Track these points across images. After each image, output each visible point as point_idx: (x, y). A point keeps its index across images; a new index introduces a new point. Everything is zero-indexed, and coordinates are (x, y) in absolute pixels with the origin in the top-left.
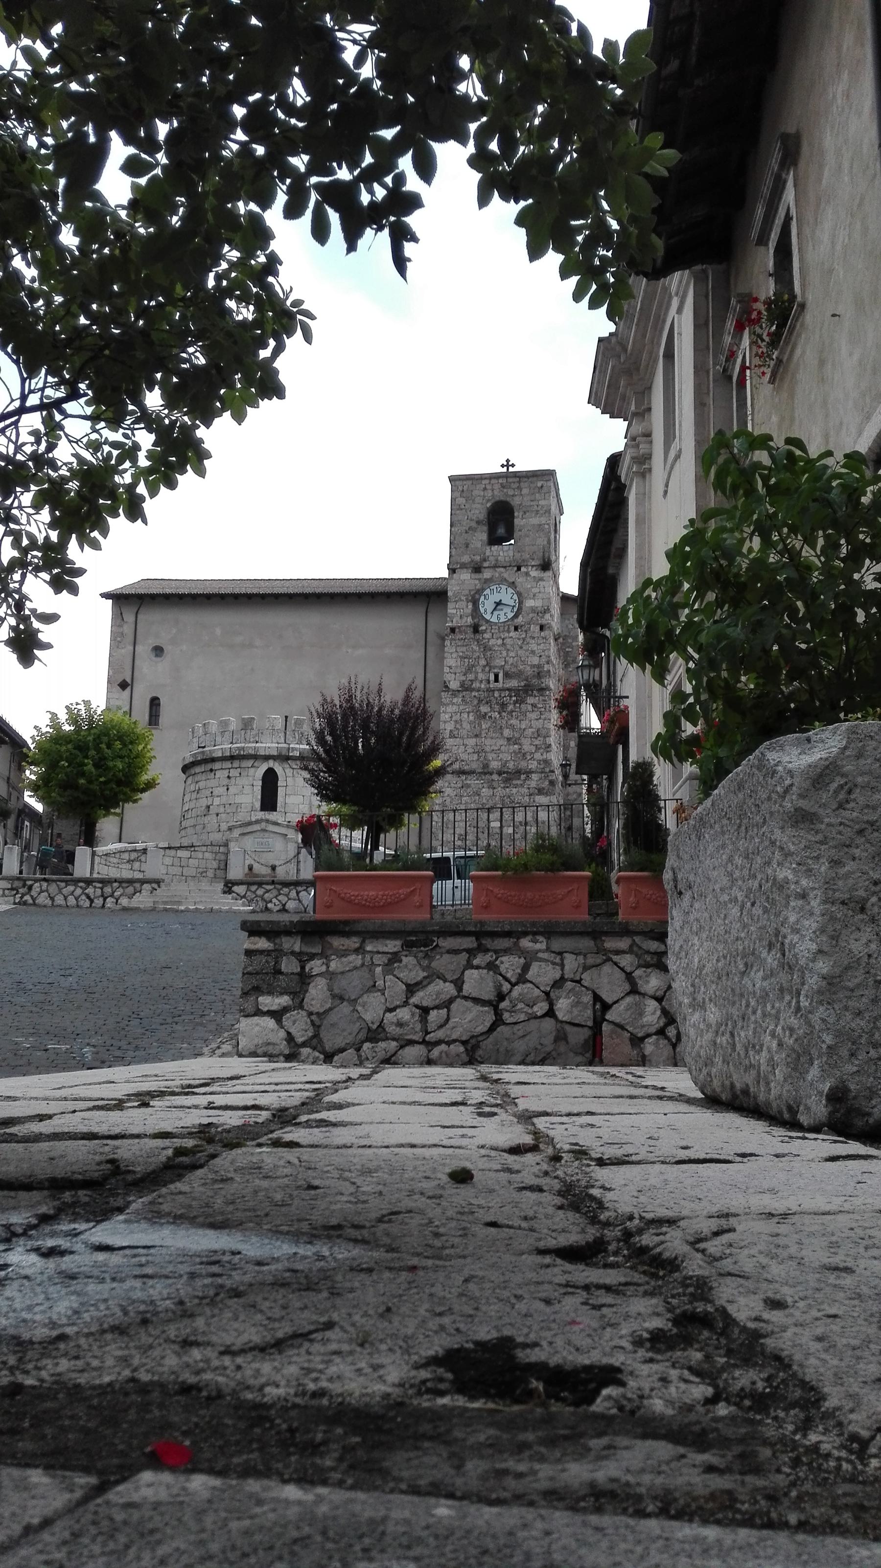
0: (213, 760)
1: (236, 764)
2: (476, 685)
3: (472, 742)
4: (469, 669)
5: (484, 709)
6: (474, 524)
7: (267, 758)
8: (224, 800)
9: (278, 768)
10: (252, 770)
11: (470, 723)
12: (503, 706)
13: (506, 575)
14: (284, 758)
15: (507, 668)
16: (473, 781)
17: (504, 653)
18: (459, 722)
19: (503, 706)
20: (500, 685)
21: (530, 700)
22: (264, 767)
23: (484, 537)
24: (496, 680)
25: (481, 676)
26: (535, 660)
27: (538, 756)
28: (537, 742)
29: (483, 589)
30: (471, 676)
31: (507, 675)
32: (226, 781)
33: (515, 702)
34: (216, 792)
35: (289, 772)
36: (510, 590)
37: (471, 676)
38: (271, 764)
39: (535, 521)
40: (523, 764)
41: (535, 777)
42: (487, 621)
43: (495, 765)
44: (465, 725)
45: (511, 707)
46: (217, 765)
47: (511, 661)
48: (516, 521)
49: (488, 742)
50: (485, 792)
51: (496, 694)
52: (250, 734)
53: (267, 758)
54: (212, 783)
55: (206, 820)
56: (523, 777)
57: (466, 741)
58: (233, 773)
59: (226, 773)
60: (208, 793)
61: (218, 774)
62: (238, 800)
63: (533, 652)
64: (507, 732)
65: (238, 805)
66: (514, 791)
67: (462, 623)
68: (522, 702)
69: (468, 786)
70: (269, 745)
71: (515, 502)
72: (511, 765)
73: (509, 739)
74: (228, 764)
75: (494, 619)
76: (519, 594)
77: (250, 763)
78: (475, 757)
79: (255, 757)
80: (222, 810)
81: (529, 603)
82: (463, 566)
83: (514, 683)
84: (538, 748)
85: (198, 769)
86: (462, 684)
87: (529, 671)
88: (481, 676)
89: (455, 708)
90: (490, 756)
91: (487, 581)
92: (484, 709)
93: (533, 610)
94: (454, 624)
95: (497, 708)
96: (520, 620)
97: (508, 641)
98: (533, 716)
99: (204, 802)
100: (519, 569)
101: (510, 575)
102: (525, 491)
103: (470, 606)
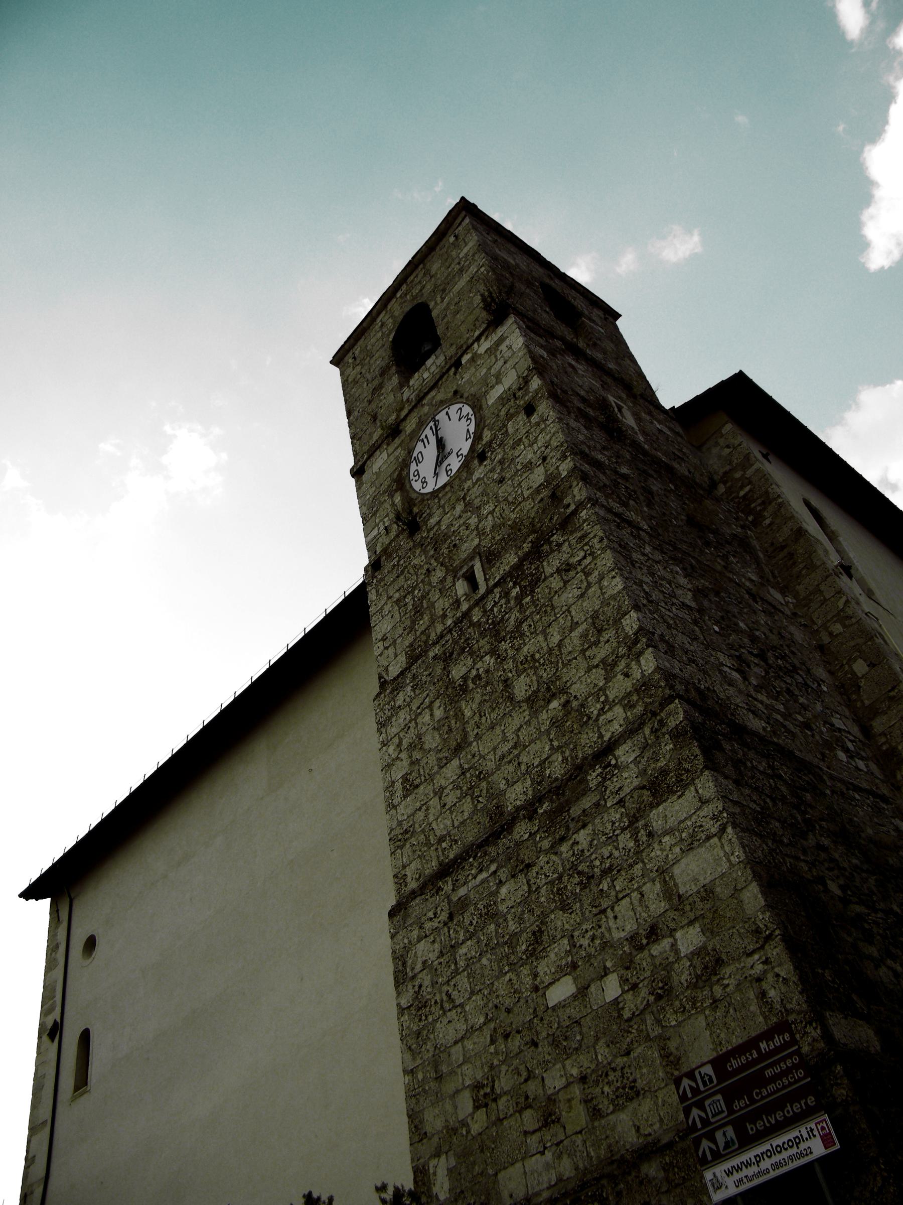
3: (451, 770)
4: (418, 611)
5: (457, 672)
12: (496, 631)
15: (486, 542)
16: (471, 884)
18: (417, 744)
19: (496, 631)
21: (550, 566)
26: (538, 476)
27: (620, 686)
28: (601, 652)
40: (588, 740)
41: (625, 754)
43: (516, 795)
44: (432, 741)
47: (489, 523)
50: (510, 893)
56: (593, 778)
63: (529, 467)
64: (521, 687)
66: (583, 837)
68: (536, 581)
69: (464, 903)
72: (557, 769)
73: (531, 700)
84: (609, 666)
96: (487, 435)
98: (571, 593)
100: (457, 364)
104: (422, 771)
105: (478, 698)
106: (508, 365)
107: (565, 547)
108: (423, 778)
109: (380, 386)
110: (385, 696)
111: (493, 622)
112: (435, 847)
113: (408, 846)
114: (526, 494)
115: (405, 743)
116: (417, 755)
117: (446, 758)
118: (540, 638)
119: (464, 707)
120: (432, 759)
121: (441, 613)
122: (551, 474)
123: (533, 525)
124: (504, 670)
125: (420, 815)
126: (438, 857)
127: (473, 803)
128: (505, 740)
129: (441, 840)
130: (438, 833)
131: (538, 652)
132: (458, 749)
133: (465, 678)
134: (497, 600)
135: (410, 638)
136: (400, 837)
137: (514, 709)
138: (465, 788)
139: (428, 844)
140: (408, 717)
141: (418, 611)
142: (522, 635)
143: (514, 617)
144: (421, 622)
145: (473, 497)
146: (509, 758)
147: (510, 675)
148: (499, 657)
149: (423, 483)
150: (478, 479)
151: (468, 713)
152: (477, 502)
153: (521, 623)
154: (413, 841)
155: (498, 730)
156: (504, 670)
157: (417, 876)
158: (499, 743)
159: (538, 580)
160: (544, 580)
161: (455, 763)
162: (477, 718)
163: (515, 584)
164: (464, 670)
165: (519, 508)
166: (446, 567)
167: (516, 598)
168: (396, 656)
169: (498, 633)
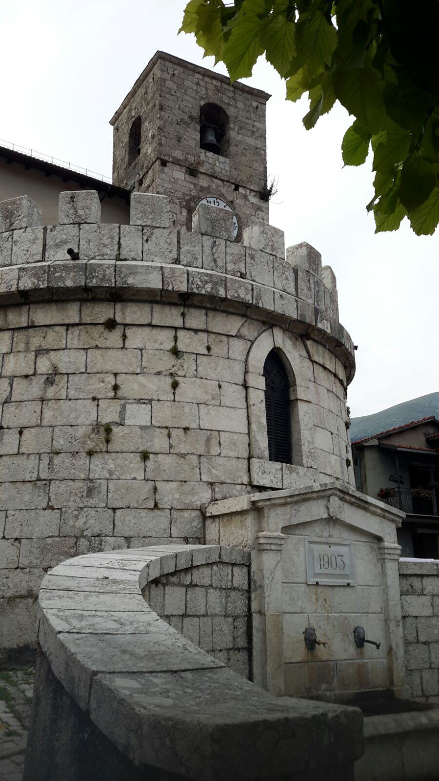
1: (196, 319)
7: (271, 321)
8: (164, 414)
10: (238, 348)
13: (223, 190)
29: (200, 199)
32: (167, 362)
34: (131, 387)
46: (133, 313)
53: (271, 321)
54: (114, 360)
55: (99, 467)
59: (165, 339)
60: (103, 388)
61: (136, 338)
62: (212, 419)
65: (212, 436)
71: (231, 111)
77: (233, 325)
80: (159, 442)
82: (177, 162)
85: (43, 315)
91: (202, 189)
99: (86, 415)
100: (236, 188)
101: (227, 190)
102: (240, 105)
103: (185, 213)
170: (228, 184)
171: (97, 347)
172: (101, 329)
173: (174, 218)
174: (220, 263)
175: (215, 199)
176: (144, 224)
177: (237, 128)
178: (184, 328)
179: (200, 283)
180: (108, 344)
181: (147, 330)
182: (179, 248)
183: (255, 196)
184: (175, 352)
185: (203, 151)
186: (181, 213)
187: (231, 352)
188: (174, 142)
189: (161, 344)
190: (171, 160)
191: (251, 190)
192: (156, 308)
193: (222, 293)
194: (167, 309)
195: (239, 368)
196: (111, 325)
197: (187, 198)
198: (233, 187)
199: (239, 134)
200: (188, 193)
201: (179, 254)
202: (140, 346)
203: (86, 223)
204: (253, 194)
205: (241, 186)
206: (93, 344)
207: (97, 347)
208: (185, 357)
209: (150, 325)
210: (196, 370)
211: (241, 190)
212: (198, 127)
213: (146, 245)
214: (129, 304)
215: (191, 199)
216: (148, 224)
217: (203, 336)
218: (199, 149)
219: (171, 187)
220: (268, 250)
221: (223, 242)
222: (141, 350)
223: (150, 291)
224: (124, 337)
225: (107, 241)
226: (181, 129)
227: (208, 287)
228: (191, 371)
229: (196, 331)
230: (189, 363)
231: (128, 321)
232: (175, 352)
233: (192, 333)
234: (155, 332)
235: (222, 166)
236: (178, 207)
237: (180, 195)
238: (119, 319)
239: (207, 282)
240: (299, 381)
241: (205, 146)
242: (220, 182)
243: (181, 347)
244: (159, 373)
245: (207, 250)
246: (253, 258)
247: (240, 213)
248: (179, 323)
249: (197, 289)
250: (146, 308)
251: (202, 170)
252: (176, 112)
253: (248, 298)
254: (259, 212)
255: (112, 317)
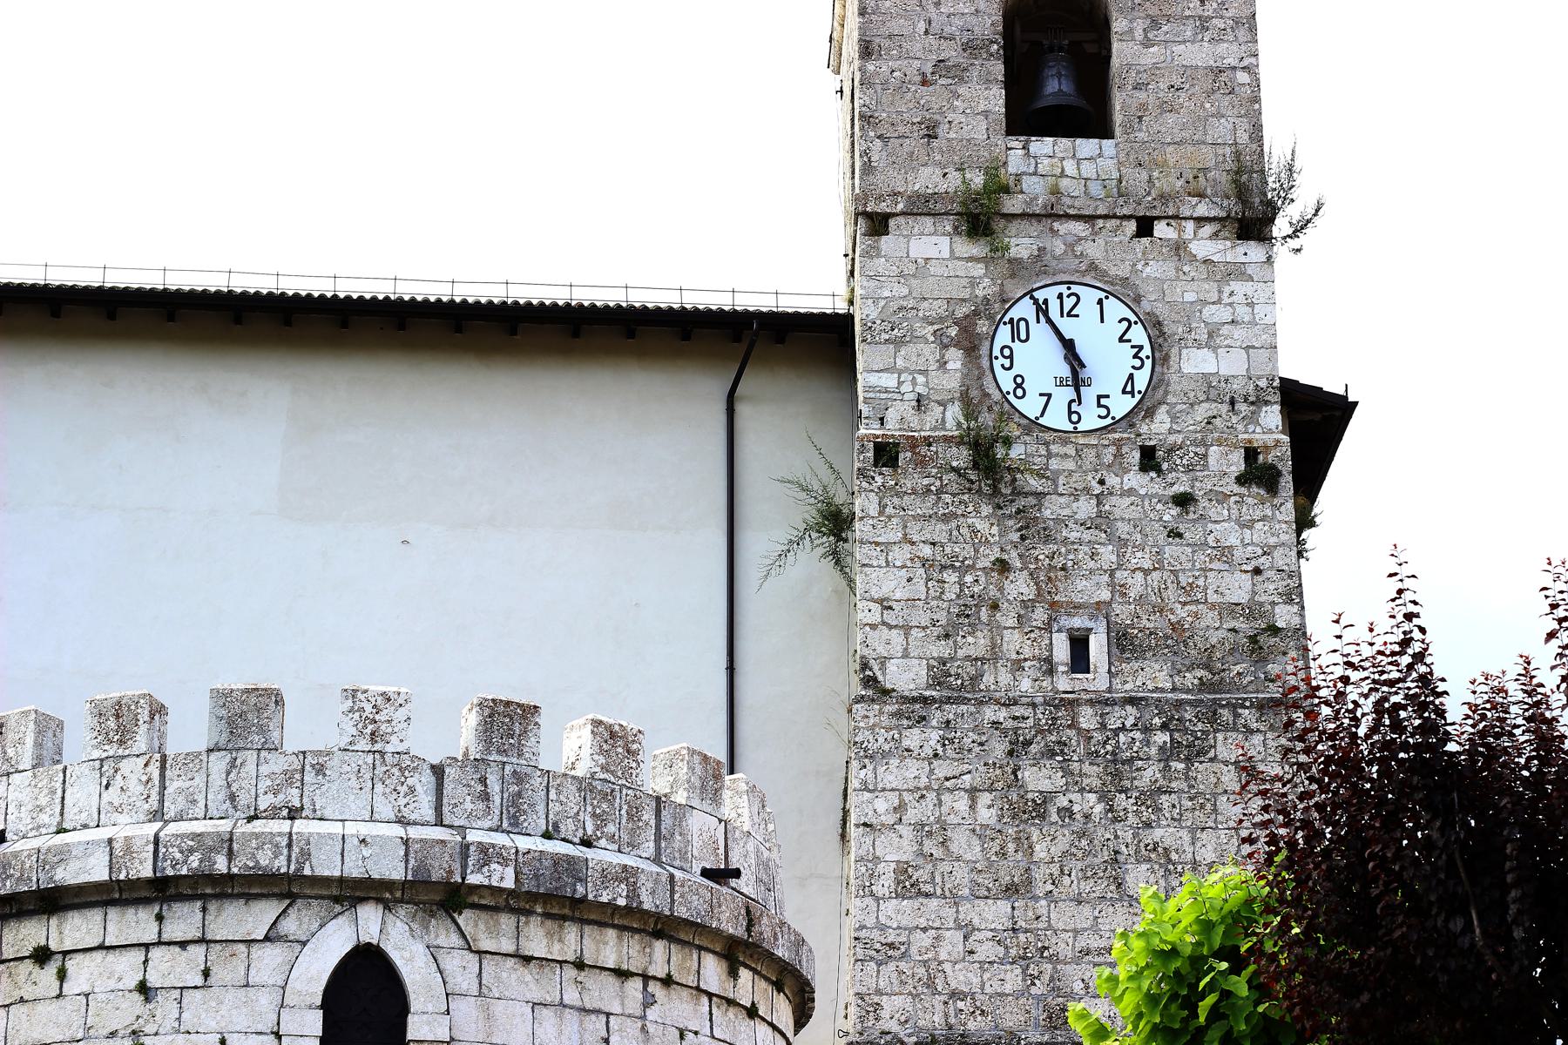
0: (54, 901)
1: (184, 920)
2: (997, 679)
3: (996, 913)
4: (965, 616)
5: (1038, 778)
6: (952, 53)
7: (350, 893)
9: (407, 945)
10: (269, 959)
11: (980, 833)
12: (1118, 768)
13: (1095, 250)
14: (440, 897)
15: (1122, 613)
17: (1108, 555)
19: (1118, 768)
20: (1097, 680)
22: (333, 942)
23: (996, 100)
24: (1080, 660)
25: (1013, 642)
26: (1238, 588)
29: (1007, 302)
30: (977, 644)
31: (1122, 643)
33: (1167, 754)
35: (461, 968)
36: (1115, 309)
37: (977, 644)
38: (370, 923)
39: (1199, 54)
42: (1032, 426)
44: (960, 841)
45: (1150, 774)
46: (76, 929)
48: (1122, 53)
49: (1064, 916)
51: (1087, 718)
52: (259, 775)
53: (350, 893)
57: (968, 912)
58: (167, 968)
59: (127, 967)
61: (82, 972)
63: (1224, 553)
67: (925, 425)
68: (1196, 752)
70: (356, 830)
74: (137, 924)
75: (1056, 418)
76: (1154, 326)
77: (258, 917)
78: (1013, 979)
79: (288, 887)
81: (1195, 362)
82: (922, 207)
83: (1154, 676)
86: (940, 674)
87: (1213, 630)
88: (1013, 642)
89: (913, 771)
90: (1074, 977)
92: (1038, 778)
93: (1211, 387)
94: (893, 428)
95: (1093, 774)
97: (1120, 506)
100: (1145, 227)
101: (1110, 247)
104: (938, 879)
105: (1063, 843)
106: (1238, 333)
107: (1257, 739)
108: (939, 892)
109: (958, 74)
110: (881, 712)
111: (1114, 753)
112: (944, 998)
113: (892, 966)
114: (1213, 598)
115: (912, 815)
116: (929, 846)
117: (989, 890)
118: (1186, 837)
119: (1034, 838)
120: (962, 875)
121: (1014, 656)
122: (1261, 604)
123: (1210, 657)
124: (1117, 837)
125: (924, 940)
126: (946, 1015)
127: (1024, 980)
128: (1095, 928)
129: (955, 995)
130: (953, 985)
131: (1177, 851)
132: (1011, 891)
133: (1047, 797)
134: (1128, 724)
135: (942, 649)
136: (878, 946)
137: (1121, 900)
138: (1013, 952)
139: (930, 983)
140: (924, 781)
141: (965, 616)
142: (1158, 810)
143: (1150, 774)
144: (970, 639)
145: (1117, 513)
146: (1097, 959)
147: (1123, 848)
148: (1111, 810)
149: (1019, 386)
150: (1131, 492)
151: (1040, 851)
152: (1123, 529)
153: (1161, 791)
154: (903, 965)
155: (1086, 910)
156: (1117, 837)
157: (903, 1019)
158: (1085, 930)
159: (1201, 752)
160: (1211, 760)
161: (1004, 906)
162: (1055, 869)
163: (1164, 727)
164: (1046, 785)
165: (1193, 608)
166: (1039, 589)
167: (1162, 749)
168: (906, 655)
169: (1117, 775)
170: (1114, 222)
171: (22, 1000)
172: (28, 965)
173: (919, 389)
174: (244, 799)
175: (1063, 289)
176: (105, 755)
177: (1139, 26)
178: (160, 943)
179: (178, 856)
180: (39, 992)
181: (98, 955)
182: (163, 787)
183: (1215, 235)
184: (143, 989)
185: (1016, 142)
186: (943, 364)
187: (252, 972)
188: (914, 144)
189: (120, 979)
190: (900, 207)
191: (1201, 221)
192: (113, 913)
193: (221, 865)
194: (131, 911)
195: (265, 1002)
196: (42, 956)
197: (962, 311)
198: (1131, 226)
199: (1148, 43)
200: (966, 294)
201: (162, 801)
202: (86, 988)
203: (17, 771)
204: (1208, 229)
205: (1159, 218)
206: (17, 995)
207: (22, 1000)
208: (159, 998)
209: (101, 947)
210: (179, 1019)
211: (1160, 229)
212: (998, 69)
213: (105, 795)
214: (70, 914)
215: (976, 313)
216: (111, 753)
217: (197, 951)
218: (1000, 140)
219: (905, 291)
220: (363, 744)
221: (251, 756)
222: (87, 995)
223: (97, 887)
224: (62, 975)
225: (43, 801)
226: (933, 97)
227: (194, 861)
228: (170, 1023)
229: (183, 945)
230: (165, 1006)
231: (68, 946)
232: (143, 989)
233: (177, 949)
234: (111, 957)
235: (1088, 170)
236: (930, 352)
237: (938, 308)
238: (53, 946)
239: (191, 851)
240: (416, 1003)
241: (1026, 117)
242: (1079, 228)
243: (154, 980)
244: (113, 1034)
245: (218, 780)
246: (320, 770)
247: (1161, 310)
248: (150, 935)
249: (173, 867)
250: (95, 915)
251: (1012, 205)
252: (916, 48)
253: (281, 865)
254: (1235, 286)
255: (43, 943)
